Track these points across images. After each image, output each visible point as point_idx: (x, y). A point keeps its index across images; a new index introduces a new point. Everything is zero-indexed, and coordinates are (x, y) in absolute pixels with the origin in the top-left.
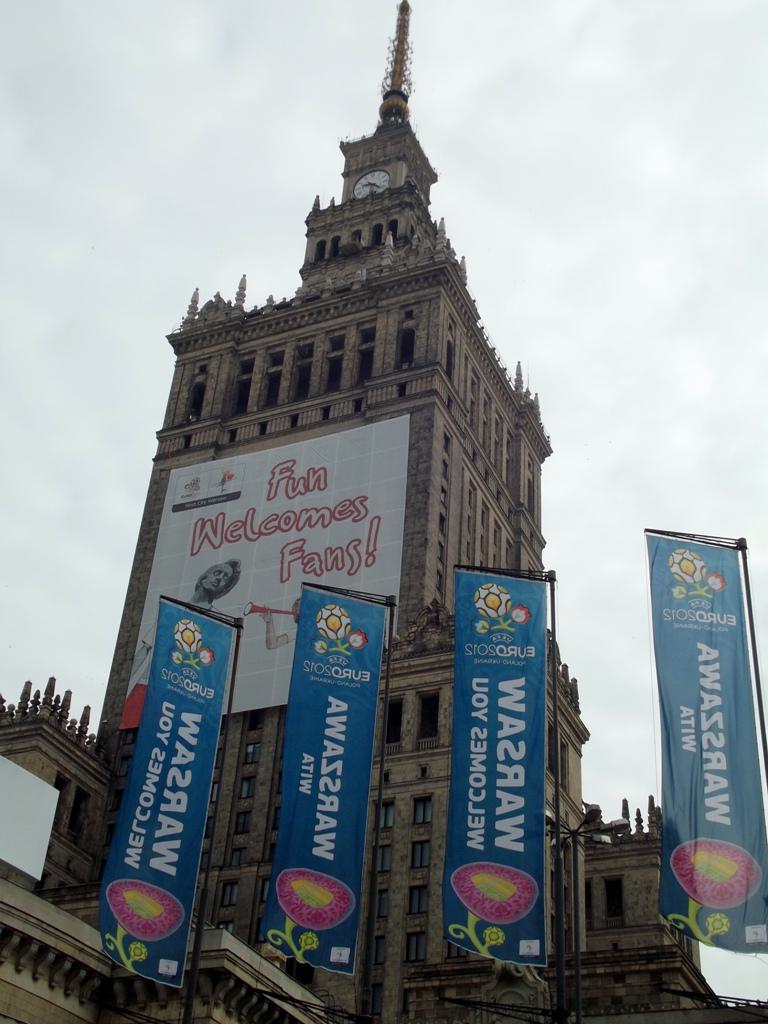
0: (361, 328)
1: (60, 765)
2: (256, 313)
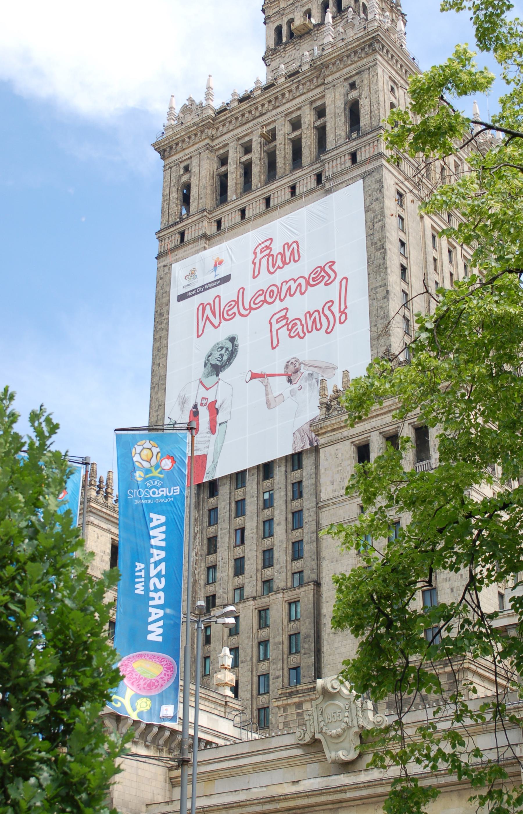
0: (314, 106)
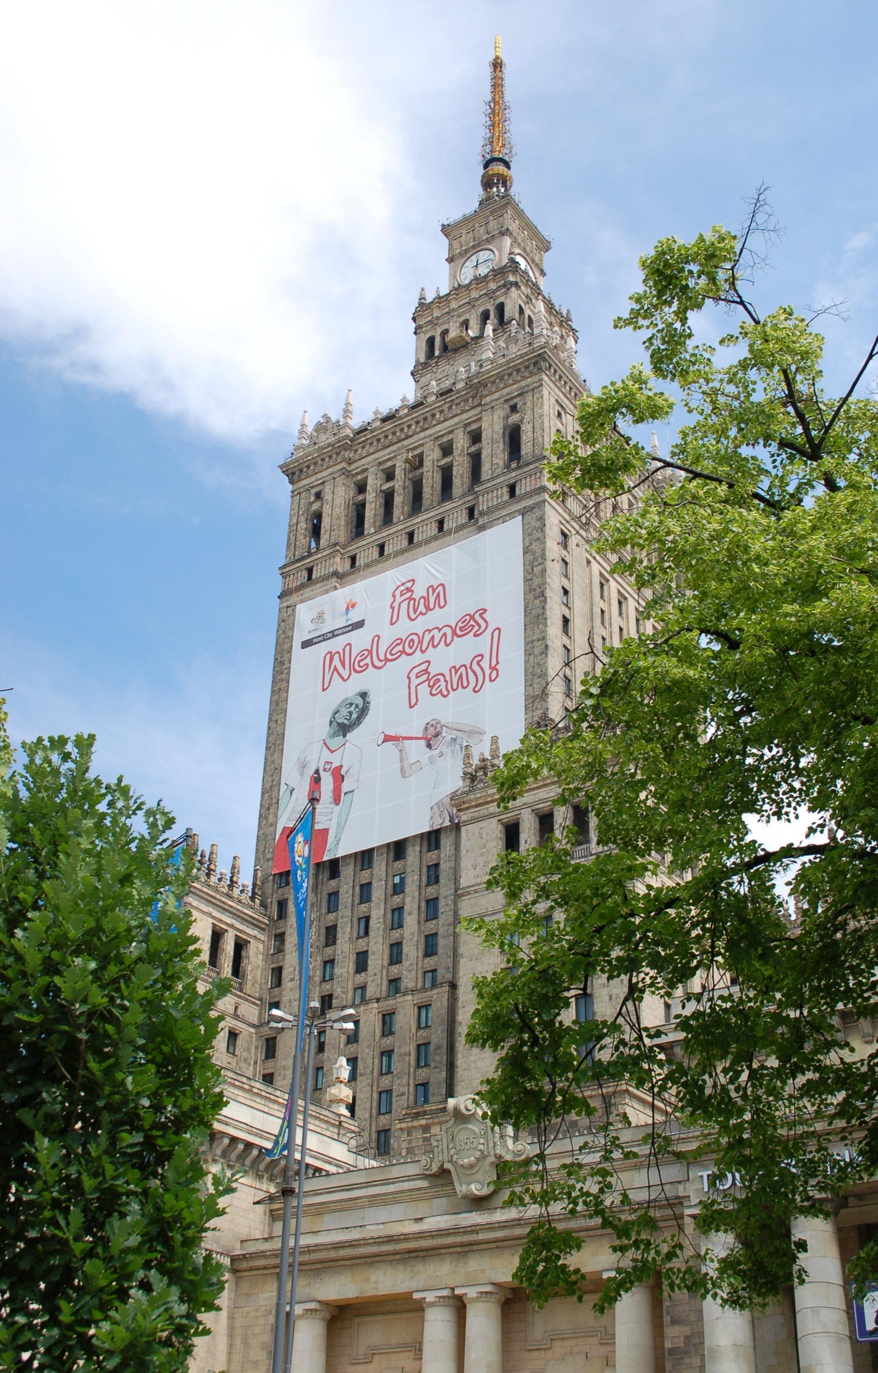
0: (469, 429)
1: (213, 917)
2: (363, 430)
